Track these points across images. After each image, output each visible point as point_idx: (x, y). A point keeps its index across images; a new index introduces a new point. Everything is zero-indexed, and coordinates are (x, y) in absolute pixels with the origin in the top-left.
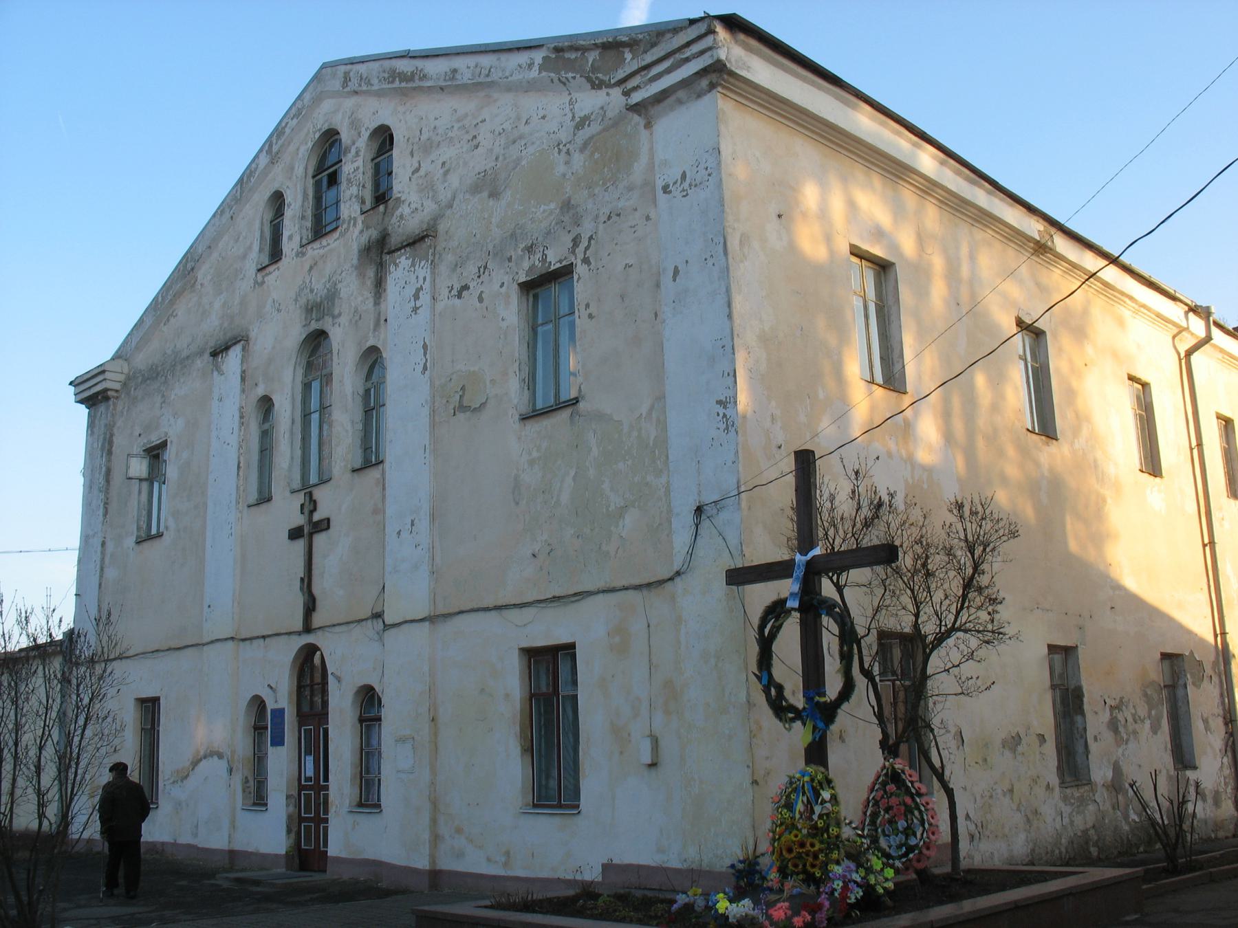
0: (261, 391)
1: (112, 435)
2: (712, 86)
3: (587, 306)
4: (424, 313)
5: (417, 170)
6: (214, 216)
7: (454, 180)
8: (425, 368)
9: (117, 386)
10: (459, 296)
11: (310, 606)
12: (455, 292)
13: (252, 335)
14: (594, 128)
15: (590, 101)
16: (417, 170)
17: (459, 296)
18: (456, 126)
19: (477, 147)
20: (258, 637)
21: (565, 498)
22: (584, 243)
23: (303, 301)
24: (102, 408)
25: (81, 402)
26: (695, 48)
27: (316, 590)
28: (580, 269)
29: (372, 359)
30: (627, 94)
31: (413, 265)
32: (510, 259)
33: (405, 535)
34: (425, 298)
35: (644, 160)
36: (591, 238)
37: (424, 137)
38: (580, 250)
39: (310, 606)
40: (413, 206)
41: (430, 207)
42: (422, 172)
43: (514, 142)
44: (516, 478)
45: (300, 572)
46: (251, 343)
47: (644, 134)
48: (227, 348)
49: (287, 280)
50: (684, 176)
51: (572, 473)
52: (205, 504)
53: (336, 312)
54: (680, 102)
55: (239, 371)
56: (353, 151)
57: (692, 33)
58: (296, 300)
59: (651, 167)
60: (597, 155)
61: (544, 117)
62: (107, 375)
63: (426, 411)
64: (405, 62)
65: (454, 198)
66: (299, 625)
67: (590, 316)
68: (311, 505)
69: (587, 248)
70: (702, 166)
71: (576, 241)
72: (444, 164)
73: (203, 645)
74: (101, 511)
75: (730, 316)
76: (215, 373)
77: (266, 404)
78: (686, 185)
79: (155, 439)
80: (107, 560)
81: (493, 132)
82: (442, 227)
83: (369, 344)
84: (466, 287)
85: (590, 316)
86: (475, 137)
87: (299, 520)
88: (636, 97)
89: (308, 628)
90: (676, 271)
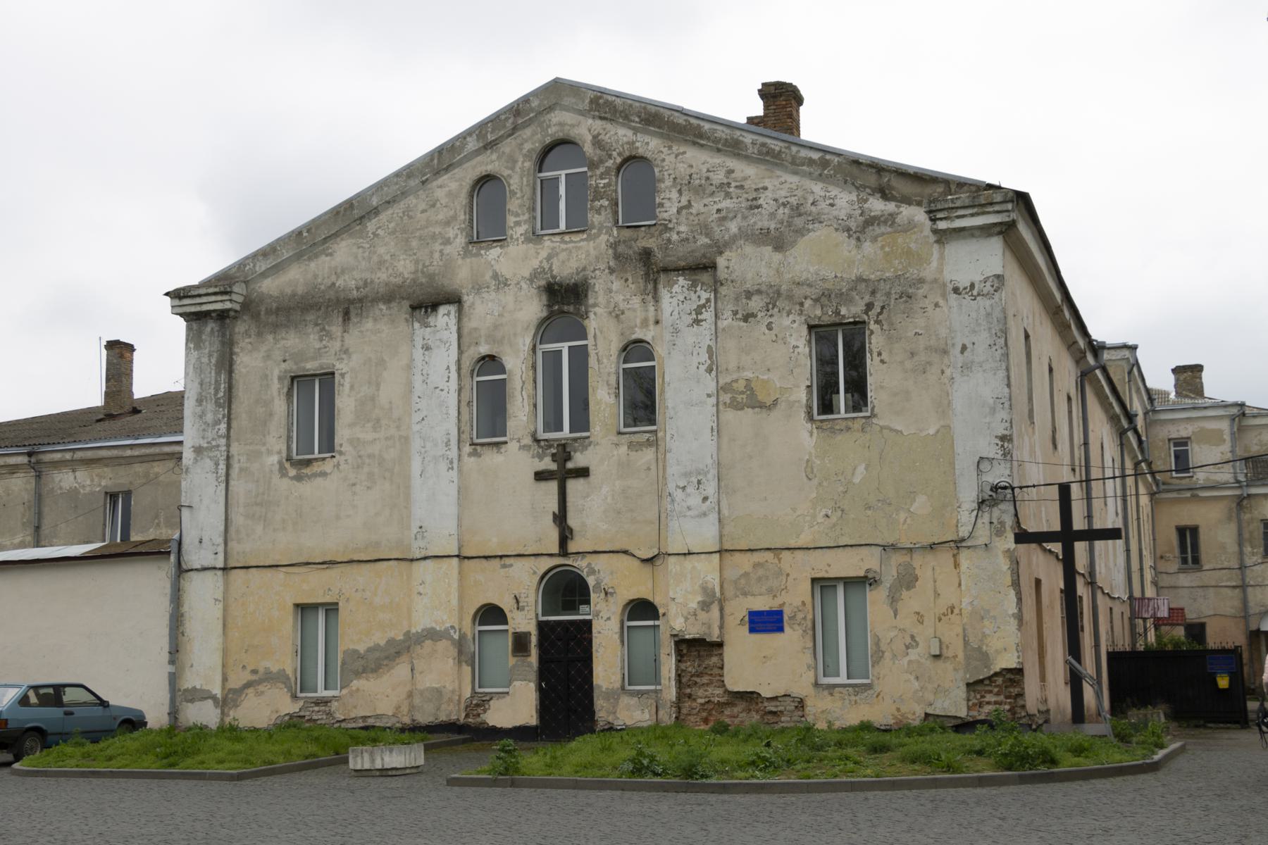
0: (484, 349)
1: (232, 353)
2: (1000, 233)
3: (879, 354)
4: (707, 326)
5: (689, 205)
6: (397, 174)
7: (733, 227)
8: (709, 370)
9: (237, 307)
10: (746, 318)
11: (565, 536)
12: (739, 316)
13: (468, 299)
14: (883, 229)
15: (877, 205)
16: (689, 205)
17: (746, 318)
18: (733, 184)
19: (758, 207)
20: (495, 557)
21: (857, 480)
22: (877, 309)
23: (543, 283)
24: (211, 326)
25: (181, 315)
26: (997, 208)
27: (572, 521)
28: (873, 326)
29: (635, 349)
30: (933, 220)
31: (694, 286)
32: (802, 304)
33: (689, 490)
34: (708, 315)
35: (934, 264)
36: (883, 308)
37: (697, 182)
38: (873, 313)
39: (565, 536)
40: (683, 235)
41: (704, 240)
42: (694, 211)
43: (800, 215)
44: (808, 461)
45: (554, 506)
46: (466, 305)
47: (936, 246)
48: (434, 306)
49: (520, 260)
50: (972, 286)
51: (863, 466)
52: (406, 440)
53: (591, 301)
54: (973, 236)
55: (454, 329)
56: (602, 169)
57: (998, 198)
58: (531, 281)
59: (940, 270)
60: (887, 249)
61: (832, 205)
62: (234, 297)
63: (714, 400)
64: (676, 114)
65: (734, 239)
66: (556, 550)
67: (882, 362)
68: (563, 453)
69: (880, 313)
70: (988, 284)
71: (869, 306)
72: (719, 211)
73: (412, 560)
74: (223, 426)
75: (1009, 385)
76: (417, 325)
77: (490, 362)
78: (975, 293)
79: (311, 366)
80: (234, 472)
81: (776, 200)
82: (721, 262)
83: (634, 337)
84: (753, 315)
85: (882, 362)
86: (755, 199)
87: (548, 464)
88: (942, 225)
89: (564, 552)
90: (964, 348)
